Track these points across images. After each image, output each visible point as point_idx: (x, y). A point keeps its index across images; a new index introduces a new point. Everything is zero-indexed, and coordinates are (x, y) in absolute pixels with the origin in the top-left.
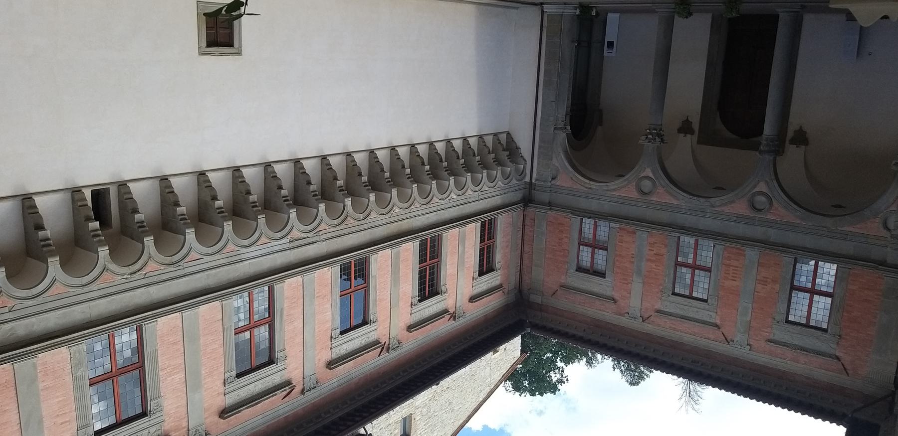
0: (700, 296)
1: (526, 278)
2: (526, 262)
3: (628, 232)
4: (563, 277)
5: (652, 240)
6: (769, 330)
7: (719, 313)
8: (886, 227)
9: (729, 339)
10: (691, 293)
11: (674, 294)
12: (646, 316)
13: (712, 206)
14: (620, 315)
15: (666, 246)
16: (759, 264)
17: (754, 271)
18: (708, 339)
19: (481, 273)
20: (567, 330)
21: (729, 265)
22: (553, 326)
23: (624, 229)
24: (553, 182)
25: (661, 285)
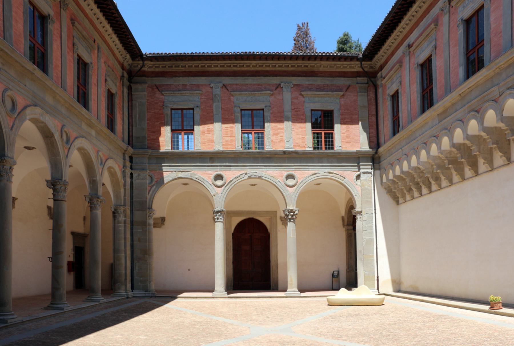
0: (246, 112)
1: (372, 95)
2: (374, 107)
3: (299, 146)
4: (342, 103)
5: (282, 144)
6: (202, 100)
7: (232, 103)
8: (151, 177)
9: (224, 88)
10: (252, 113)
11: (263, 110)
12: (278, 89)
13: (246, 174)
14: (297, 85)
15: (272, 141)
16: (213, 141)
17: (215, 137)
18: (236, 84)
19: (397, 92)
20: (333, 63)
21: (231, 136)
22: (345, 63)
23: (302, 147)
24: (358, 173)
25: (271, 114)
